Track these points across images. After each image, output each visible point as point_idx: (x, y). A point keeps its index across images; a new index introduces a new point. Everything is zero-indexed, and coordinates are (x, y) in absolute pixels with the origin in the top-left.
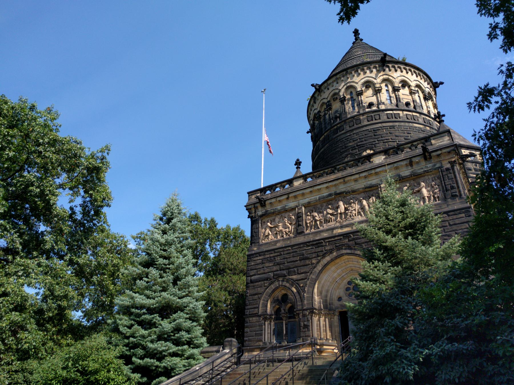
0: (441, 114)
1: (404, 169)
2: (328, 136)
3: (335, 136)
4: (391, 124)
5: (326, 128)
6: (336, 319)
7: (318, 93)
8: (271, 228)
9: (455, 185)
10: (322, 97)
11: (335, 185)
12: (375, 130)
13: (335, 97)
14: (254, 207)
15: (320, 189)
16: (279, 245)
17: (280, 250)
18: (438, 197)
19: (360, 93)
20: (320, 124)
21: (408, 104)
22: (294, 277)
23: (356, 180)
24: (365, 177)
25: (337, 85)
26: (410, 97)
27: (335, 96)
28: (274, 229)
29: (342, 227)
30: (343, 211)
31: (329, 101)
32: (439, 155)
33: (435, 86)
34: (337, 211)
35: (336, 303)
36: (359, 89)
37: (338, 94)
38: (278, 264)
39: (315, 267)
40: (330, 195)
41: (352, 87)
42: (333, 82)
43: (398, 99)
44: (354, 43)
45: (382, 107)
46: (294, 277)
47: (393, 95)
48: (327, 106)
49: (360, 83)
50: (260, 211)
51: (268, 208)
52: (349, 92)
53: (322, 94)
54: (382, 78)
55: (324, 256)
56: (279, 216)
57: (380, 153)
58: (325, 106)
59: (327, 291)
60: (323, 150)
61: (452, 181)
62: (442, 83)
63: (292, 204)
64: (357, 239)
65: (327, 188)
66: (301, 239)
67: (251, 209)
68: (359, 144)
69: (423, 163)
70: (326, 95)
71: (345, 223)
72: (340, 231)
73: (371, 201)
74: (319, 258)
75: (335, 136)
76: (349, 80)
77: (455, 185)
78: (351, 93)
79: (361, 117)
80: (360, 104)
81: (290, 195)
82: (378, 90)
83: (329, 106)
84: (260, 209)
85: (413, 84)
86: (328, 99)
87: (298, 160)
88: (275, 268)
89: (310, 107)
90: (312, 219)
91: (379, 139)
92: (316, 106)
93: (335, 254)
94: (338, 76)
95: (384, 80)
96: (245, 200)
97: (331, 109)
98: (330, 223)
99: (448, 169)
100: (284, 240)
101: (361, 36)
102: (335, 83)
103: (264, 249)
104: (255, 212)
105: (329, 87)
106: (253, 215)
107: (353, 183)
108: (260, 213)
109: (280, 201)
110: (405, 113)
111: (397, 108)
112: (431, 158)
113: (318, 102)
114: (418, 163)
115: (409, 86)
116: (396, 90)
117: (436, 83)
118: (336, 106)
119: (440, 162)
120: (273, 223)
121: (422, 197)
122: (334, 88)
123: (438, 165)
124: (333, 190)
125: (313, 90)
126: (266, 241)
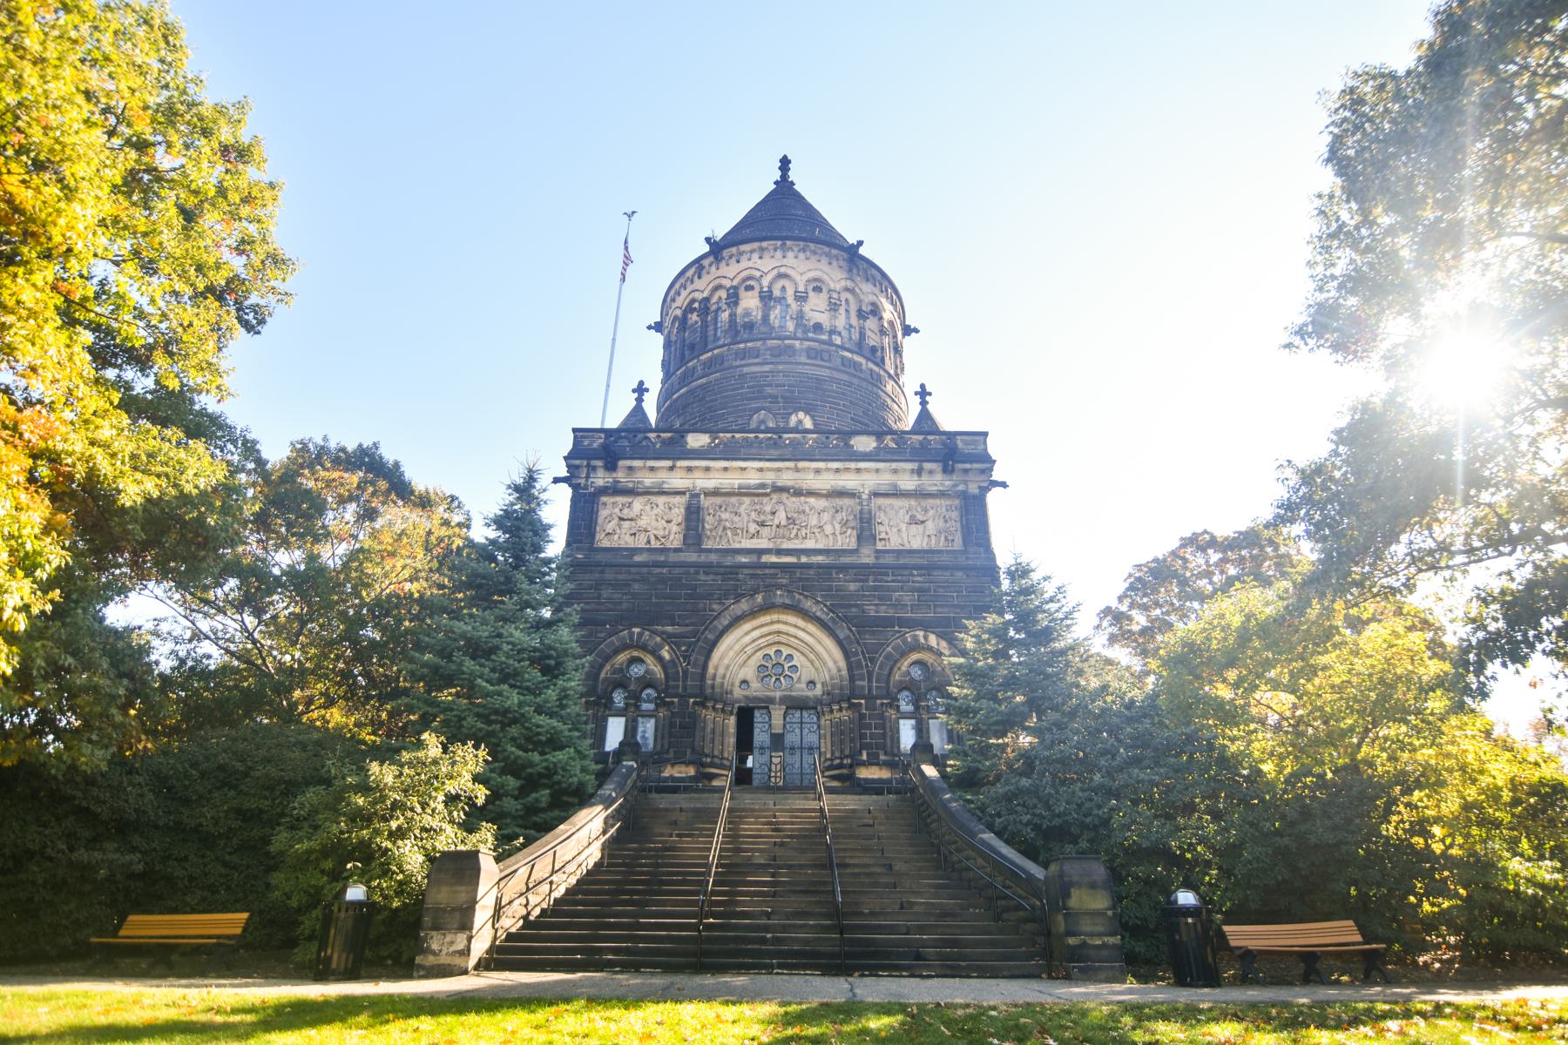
1: (907, 476)
2: (721, 356)
3: (738, 363)
4: (845, 377)
5: (716, 339)
6: (732, 721)
7: (711, 259)
10: (719, 273)
11: (779, 470)
12: (819, 380)
14: (588, 466)
16: (638, 558)
17: (644, 570)
19: (801, 298)
20: (705, 325)
21: (874, 350)
22: (669, 629)
23: (818, 471)
24: (837, 470)
26: (877, 338)
28: (626, 524)
29: (779, 552)
30: (784, 523)
31: (736, 288)
32: (966, 471)
35: (738, 693)
36: (801, 288)
37: (759, 280)
38: (634, 596)
39: (716, 618)
40: (763, 486)
41: (785, 276)
42: (752, 251)
43: (862, 335)
45: (838, 341)
46: (669, 629)
47: (854, 321)
48: (729, 297)
49: (805, 277)
50: (601, 479)
51: (620, 475)
53: (723, 264)
54: (843, 283)
55: (738, 598)
56: (641, 499)
57: (869, 433)
58: (723, 294)
59: (728, 667)
60: (704, 380)
62: (917, 331)
63: (677, 481)
64: (807, 580)
65: (761, 470)
66: (692, 557)
67: (577, 467)
69: (939, 476)
70: (730, 272)
71: (784, 546)
72: (774, 559)
73: (839, 517)
74: (728, 602)
75: (738, 363)
76: (785, 261)
78: (783, 288)
79: (797, 343)
80: (800, 316)
81: (679, 463)
83: (734, 298)
84: (601, 473)
86: (735, 283)
87: (641, 383)
88: (624, 606)
89: (682, 280)
92: (699, 284)
93: (759, 598)
94: (765, 244)
95: (847, 289)
96: (568, 446)
97: (736, 303)
98: (755, 541)
99: (975, 497)
100: (649, 550)
101: (792, 176)
102: (755, 256)
103: (599, 557)
104: (588, 477)
105: (745, 257)
106: (583, 481)
107: (811, 476)
108: (600, 482)
109: (652, 469)
110: (871, 365)
112: (953, 471)
113: (706, 278)
114: (931, 472)
115: (881, 318)
116: (861, 315)
118: (750, 302)
119: (965, 482)
120: (626, 511)
122: (750, 264)
123: (961, 487)
124: (769, 478)
125: (707, 248)
126: (606, 543)
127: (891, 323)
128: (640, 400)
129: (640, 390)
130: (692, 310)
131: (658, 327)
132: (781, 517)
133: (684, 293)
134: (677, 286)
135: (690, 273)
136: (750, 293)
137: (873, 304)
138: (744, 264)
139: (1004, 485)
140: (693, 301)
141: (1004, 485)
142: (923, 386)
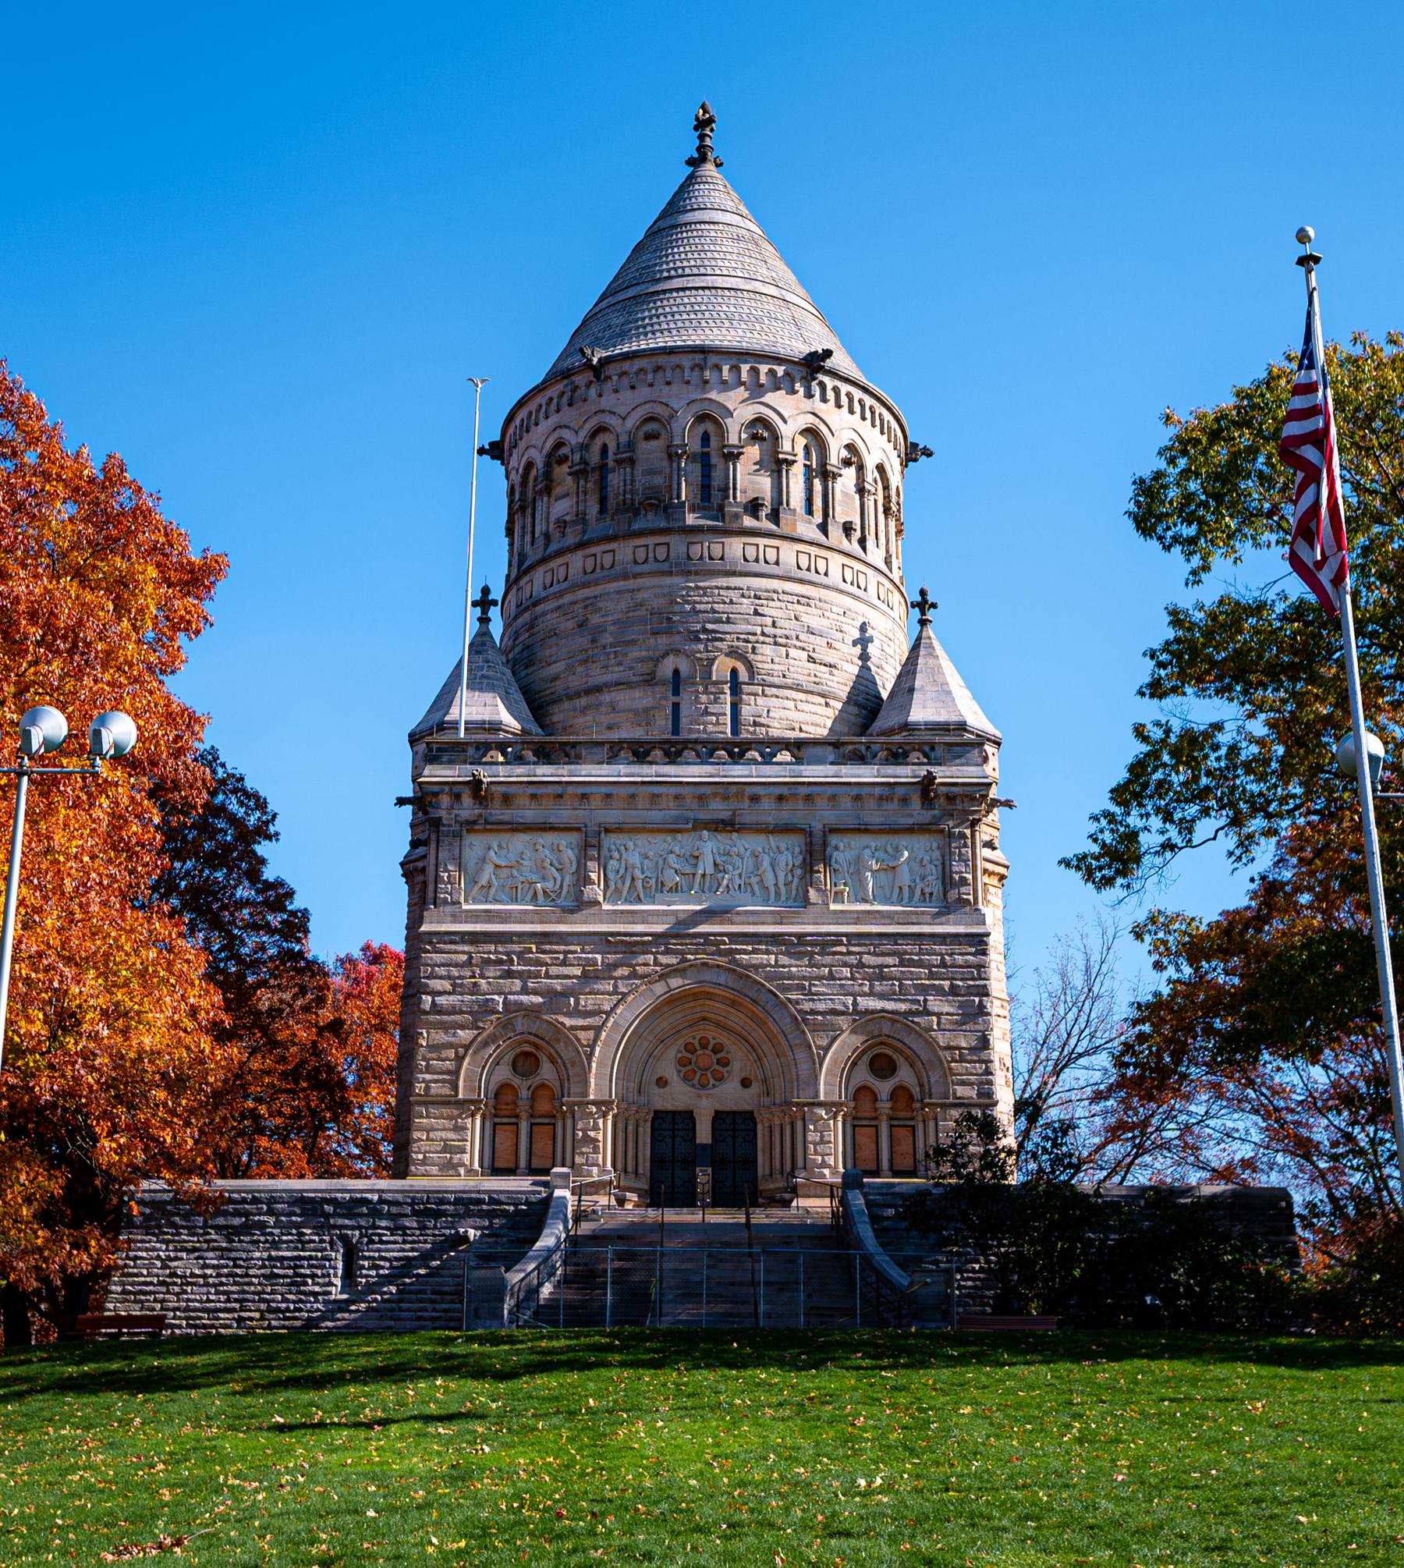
0: (930, 599)
8: (497, 866)
9: (970, 877)
10: (604, 403)
13: (652, 427)
15: (658, 796)
18: (931, 894)
21: (848, 529)
25: (666, 389)
27: (655, 425)
28: (506, 871)
30: (710, 870)
33: (912, 453)
34: (696, 865)
44: (691, 162)
52: (701, 429)
61: (967, 865)
62: (928, 453)
65: (677, 797)
68: (709, 626)
77: (970, 877)
82: (786, 461)
85: (870, 463)
87: (486, 591)
89: (541, 399)
90: (622, 871)
91: (766, 630)
111: (821, 538)
115: (861, 468)
117: (915, 446)
121: (897, 884)
127: (880, 468)
128: (484, 620)
129: (484, 602)
130: (562, 460)
131: (495, 451)
132: (706, 866)
133: (545, 426)
134: (532, 406)
135: (554, 391)
136: (654, 443)
137: (850, 447)
138: (644, 392)
139: (1008, 804)
140: (559, 444)
141: (1008, 804)
142: (923, 593)
